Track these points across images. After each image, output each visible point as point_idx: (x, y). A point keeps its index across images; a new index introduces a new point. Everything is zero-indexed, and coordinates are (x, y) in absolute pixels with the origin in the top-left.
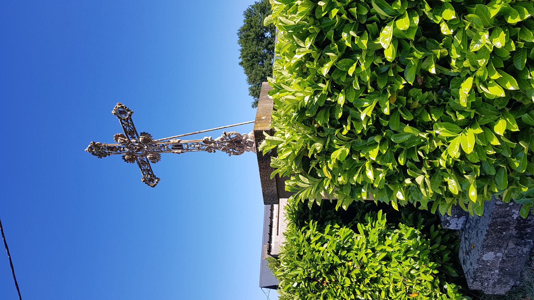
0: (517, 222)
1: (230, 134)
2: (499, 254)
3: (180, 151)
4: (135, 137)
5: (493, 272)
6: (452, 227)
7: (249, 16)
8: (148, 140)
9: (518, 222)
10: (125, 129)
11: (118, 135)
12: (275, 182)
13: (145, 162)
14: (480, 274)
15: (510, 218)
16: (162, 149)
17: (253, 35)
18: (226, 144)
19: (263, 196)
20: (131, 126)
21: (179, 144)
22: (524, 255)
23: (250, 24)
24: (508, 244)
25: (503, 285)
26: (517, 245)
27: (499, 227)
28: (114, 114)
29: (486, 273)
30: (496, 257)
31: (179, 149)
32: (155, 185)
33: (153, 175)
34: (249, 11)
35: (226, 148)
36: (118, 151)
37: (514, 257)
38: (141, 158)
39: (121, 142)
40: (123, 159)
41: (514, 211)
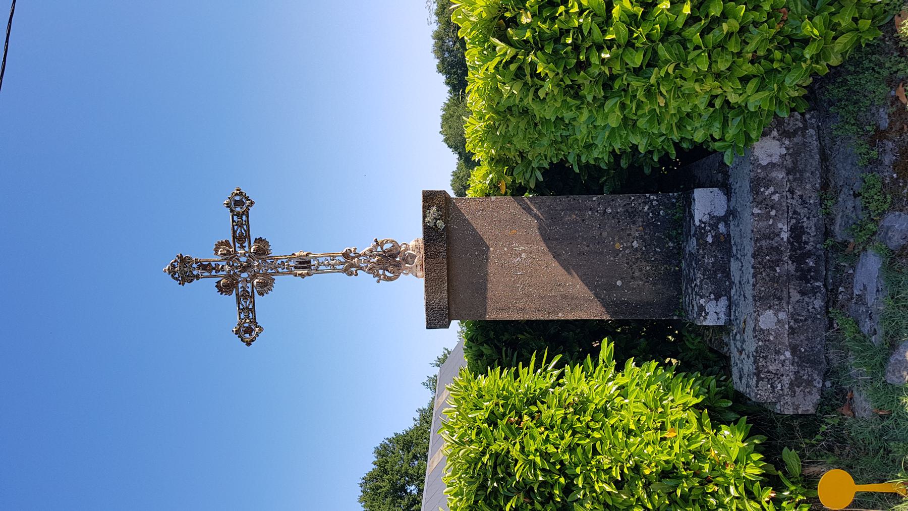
0: (789, 246)
1: (383, 241)
2: (782, 315)
3: (305, 272)
4: (245, 247)
5: (782, 358)
6: (710, 321)
7: (384, 456)
8: (262, 250)
9: (792, 247)
10: (234, 232)
11: (222, 242)
12: (446, 284)
13: (248, 293)
14: (764, 363)
15: (777, 239)
16: (280, 270)
17: (386, 485)
18: (376, 259)
19: (427, 310)
20: (245, 227)
21: (307, 260)
22: (819, 316)
23: (384, 467)
24: (789, 293)
25: (805, 387)
26: (803, 293)
27: (767, 257)
28: (227, 204)
29: (773, 360)
30: (779, 321)
31: (304, 268)
32: (252, 341)
33: (255, 319)
34: (384, 447)
35: (374, 267)
36: (214, 273)
37: (806, 320)
38: (244, 286)
39: (223, 252)
40: (216, 286)
41: (780, 225)
